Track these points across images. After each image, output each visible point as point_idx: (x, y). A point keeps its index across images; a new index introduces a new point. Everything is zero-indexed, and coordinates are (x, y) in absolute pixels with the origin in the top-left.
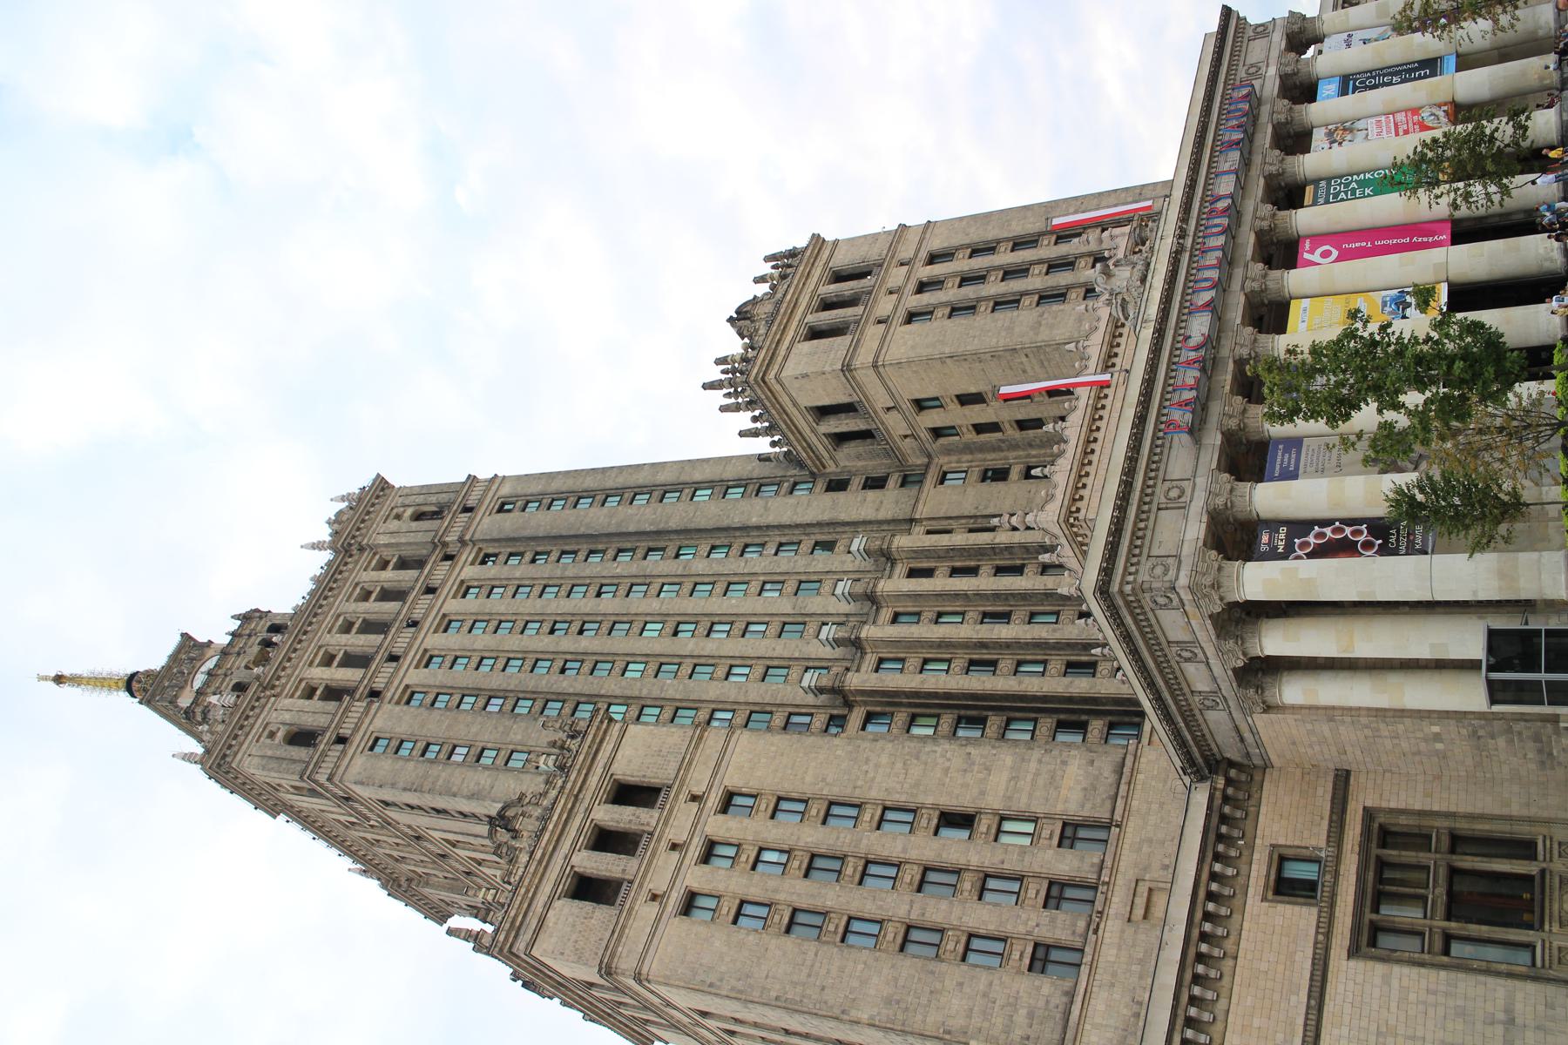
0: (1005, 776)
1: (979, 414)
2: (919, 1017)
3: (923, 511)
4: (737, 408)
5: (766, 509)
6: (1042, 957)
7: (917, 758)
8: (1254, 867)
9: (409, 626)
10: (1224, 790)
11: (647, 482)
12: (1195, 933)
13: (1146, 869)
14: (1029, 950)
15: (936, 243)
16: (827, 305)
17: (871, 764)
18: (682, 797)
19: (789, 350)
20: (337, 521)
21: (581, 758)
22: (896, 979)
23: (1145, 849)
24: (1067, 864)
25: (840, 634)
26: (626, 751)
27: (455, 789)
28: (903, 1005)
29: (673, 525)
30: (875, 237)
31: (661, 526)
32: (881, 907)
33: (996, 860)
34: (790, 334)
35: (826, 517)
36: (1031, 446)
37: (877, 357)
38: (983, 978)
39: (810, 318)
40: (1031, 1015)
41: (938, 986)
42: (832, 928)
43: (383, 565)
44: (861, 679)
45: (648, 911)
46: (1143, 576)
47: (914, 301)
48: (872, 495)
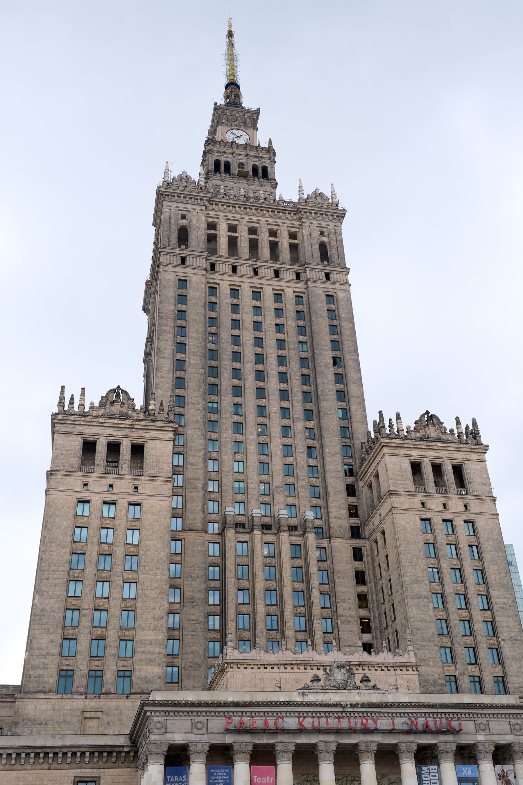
1: (384, 566)
2: (37, 626)
5: (334, 455)
6: (66, 675)
8: (90, 770)
9: (254, 269)
10: (123, 751)
11: (349, 378)
12: (57, 750)
13: (108, 715)
14: (70, 668)
15: (480, 523)
16: (437, 469)
17: (157, 571)
18: (136, 483)
19: (405, 455)
20: (318, 195)
21: (152, 424)
22: (53, 611)
23: (117, 712)
25: (256, 520)
26: (158, 444)
27: (161, 337)
28: (42, 618)
29: (323, 404)
30: (488, 484)
31: (321, 397)
32: (86, 595)
33: (111, 643)
35: (330, 490)
36: (377, 595)
37: (398, 509)
38: (56, 651)
40: (40, 676)
41: (51, 631)
42: (77, 574)
43: (293, 236)
45: (78, 485)
46: (155, 719)
47: (437, 520)
48: (345, 512)
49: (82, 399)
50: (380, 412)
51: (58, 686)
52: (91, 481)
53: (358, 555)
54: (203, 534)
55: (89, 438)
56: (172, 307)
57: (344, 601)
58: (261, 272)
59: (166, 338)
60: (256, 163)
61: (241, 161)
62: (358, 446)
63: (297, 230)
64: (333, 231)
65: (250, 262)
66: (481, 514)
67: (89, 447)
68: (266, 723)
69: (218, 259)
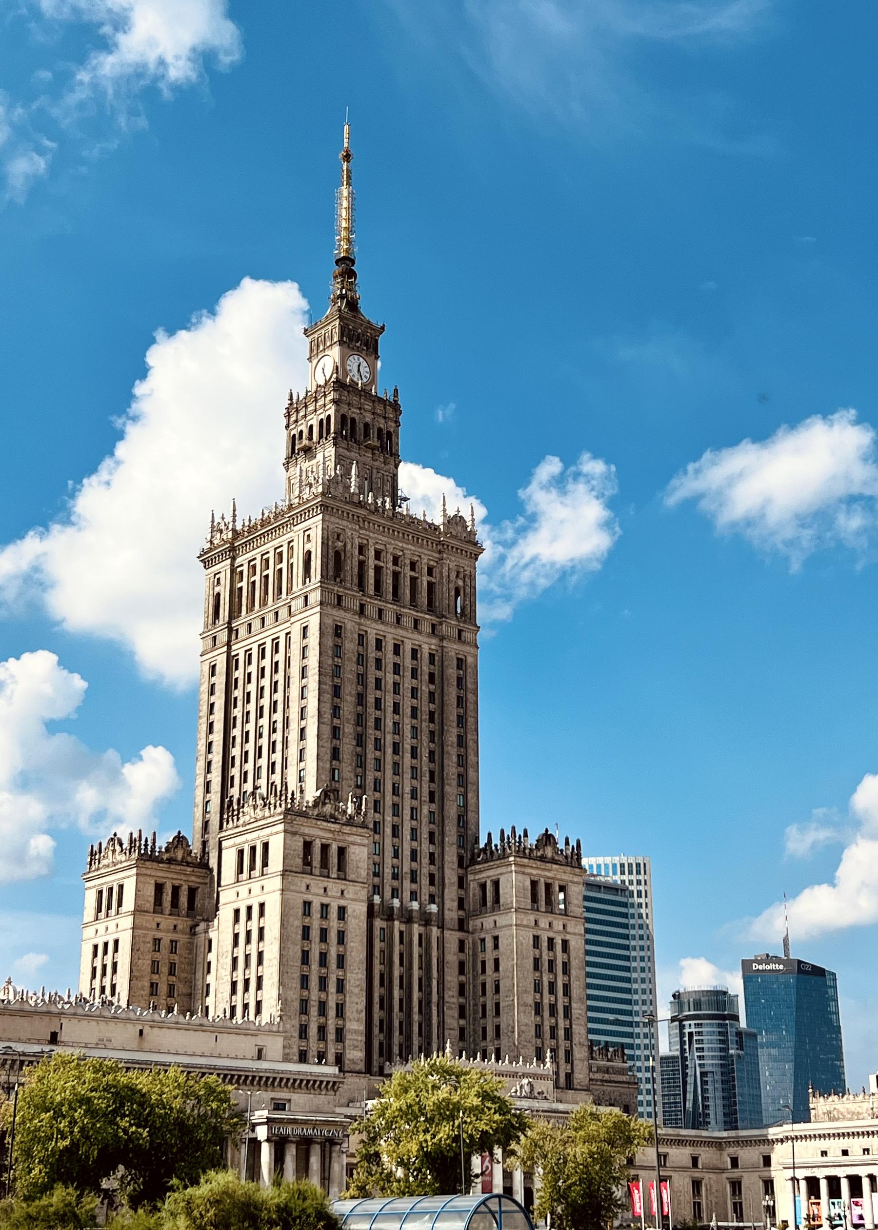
3: (447, 933)
4: (502, 839)
7: (361, 990)
11: (469, 762)
16: (548, 886)
18: (343, 887)
19: (528, 874)
21: (355, 829)
29: (447, 788)
34: (534, 872)
35: (446, 881)
36: (474, 986)
38: (296, 1034)
39: (542, 880)
43: (430, 572)
44: (378, 923)
48: (456, 904)
50: (513, 828)
55: (308, 839)
56: (330, 662)
57: (449, 989)
59: (325, 700)
60: (382, 426)
62: (471, 839)
63: (435, 564)
65: (395, 607)
66: (575, 934)
69: (368, 600)
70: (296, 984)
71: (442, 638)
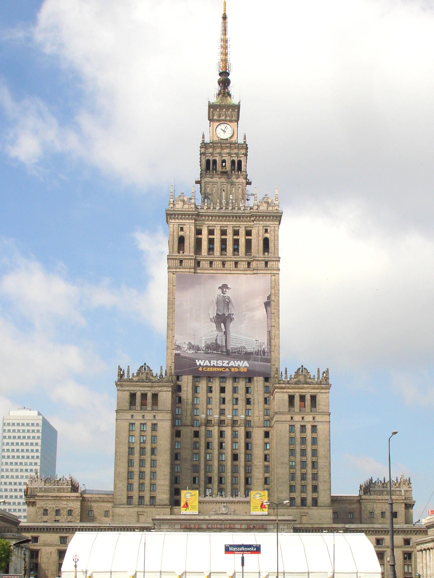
0: (163, 483)
6: (130, 498)
15: (320, 427)
18: (155, 414)
19: (286, 392)
24: (147, 499)
38: (126, 489)
40: (120, 498)
43: (248, 233)
49: (128, 372)
51: (127, 502)
52: (135, 414)
53: (267, 435)
54: (191, 427)
55: (133, 392)
58: (227, 265)
60: (234, 158)
61: (224, 158)
64: (273, 228)
66: (320, 422)
67: (133, 396)
68: (195, 526)
70: (125, 464)
71: (254, 270)
